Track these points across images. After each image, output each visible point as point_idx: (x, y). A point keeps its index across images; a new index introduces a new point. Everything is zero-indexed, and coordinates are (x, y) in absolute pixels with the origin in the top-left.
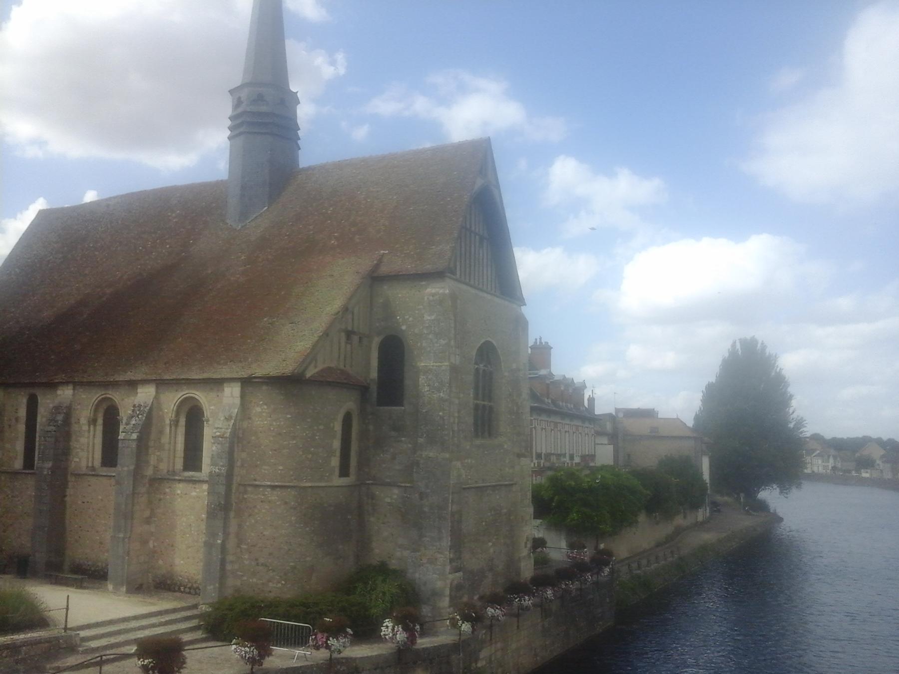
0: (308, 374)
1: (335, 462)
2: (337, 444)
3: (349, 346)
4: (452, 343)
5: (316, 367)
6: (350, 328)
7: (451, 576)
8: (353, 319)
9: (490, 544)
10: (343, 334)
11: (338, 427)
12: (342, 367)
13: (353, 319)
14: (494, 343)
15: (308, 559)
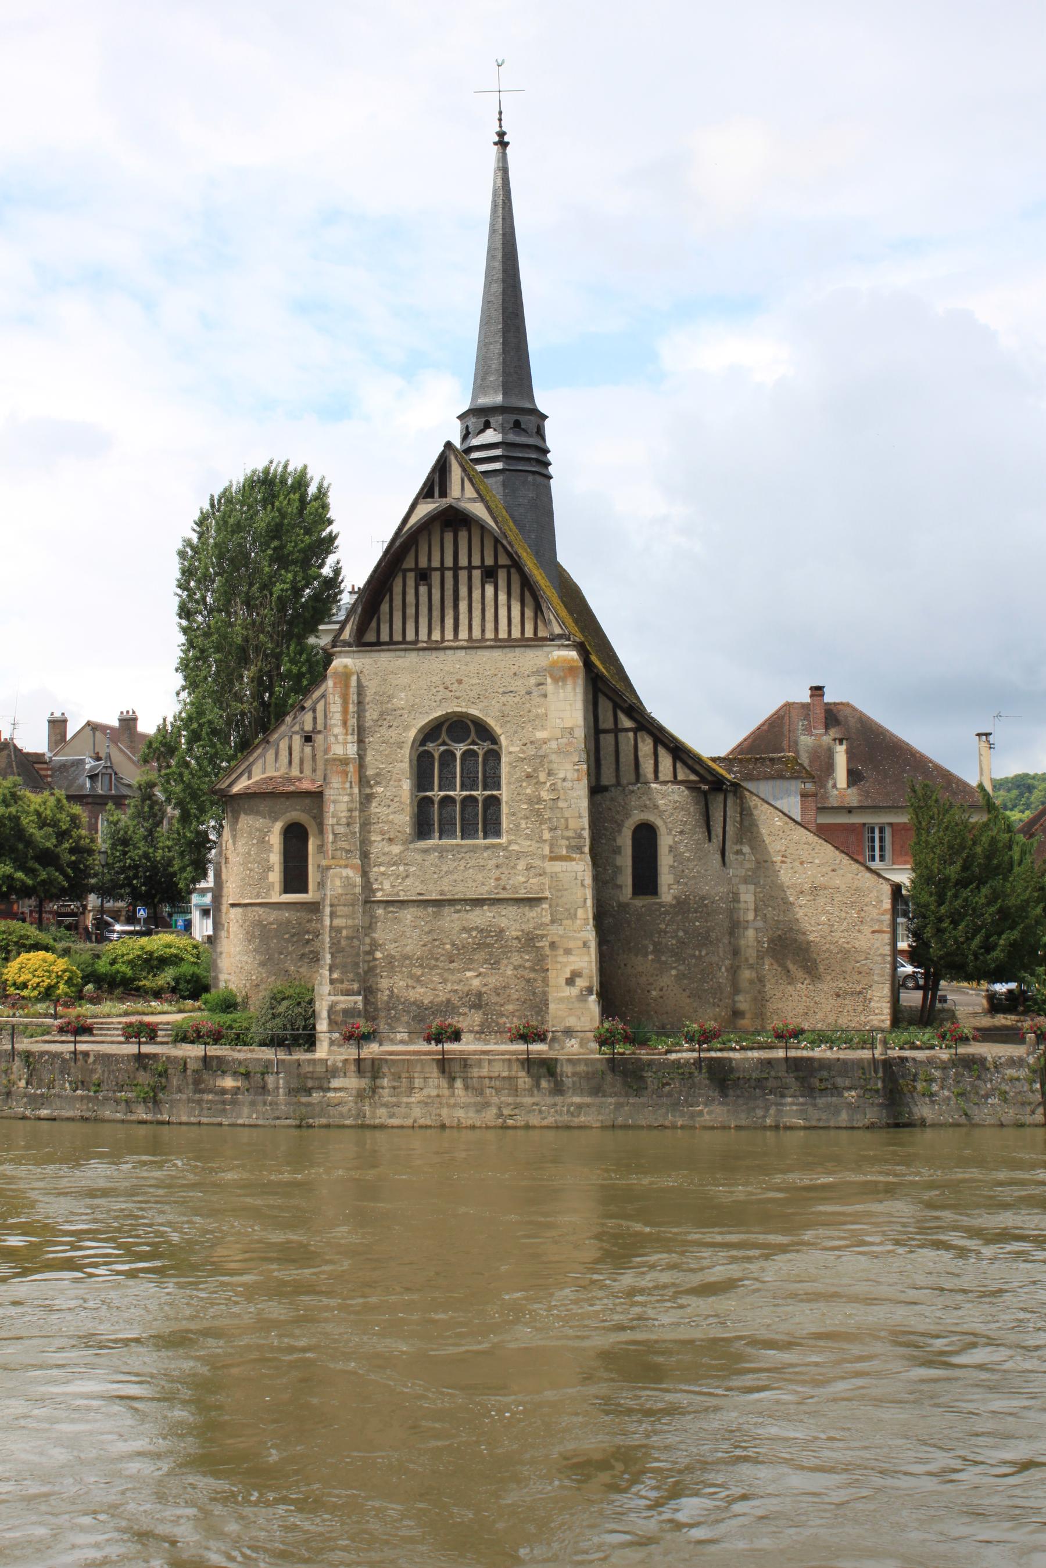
0: (236, 789)
1: (275, 877)
2: (275, 858)
3: (308, 750)
4: (338, 730)
5: (249, 778)
6: (308, 727)
7: (333, 998)
8: (315, 718)
9: (469, 974)
10: (297, 740)
11: (275, 839)
12: (295, 772)
13: (315, 718)
14: (474, 711)
15: (254, 977)
